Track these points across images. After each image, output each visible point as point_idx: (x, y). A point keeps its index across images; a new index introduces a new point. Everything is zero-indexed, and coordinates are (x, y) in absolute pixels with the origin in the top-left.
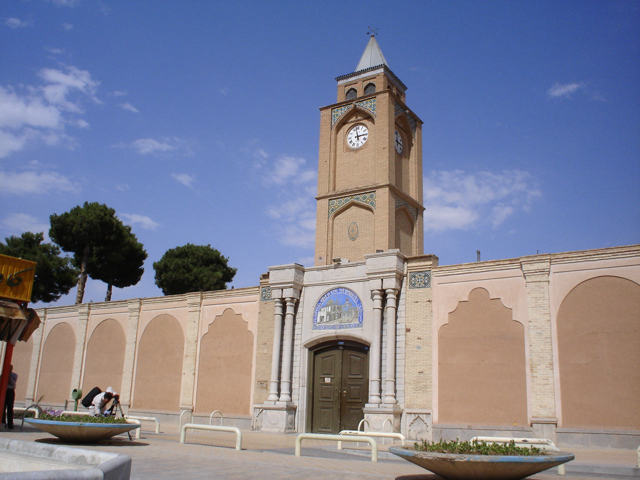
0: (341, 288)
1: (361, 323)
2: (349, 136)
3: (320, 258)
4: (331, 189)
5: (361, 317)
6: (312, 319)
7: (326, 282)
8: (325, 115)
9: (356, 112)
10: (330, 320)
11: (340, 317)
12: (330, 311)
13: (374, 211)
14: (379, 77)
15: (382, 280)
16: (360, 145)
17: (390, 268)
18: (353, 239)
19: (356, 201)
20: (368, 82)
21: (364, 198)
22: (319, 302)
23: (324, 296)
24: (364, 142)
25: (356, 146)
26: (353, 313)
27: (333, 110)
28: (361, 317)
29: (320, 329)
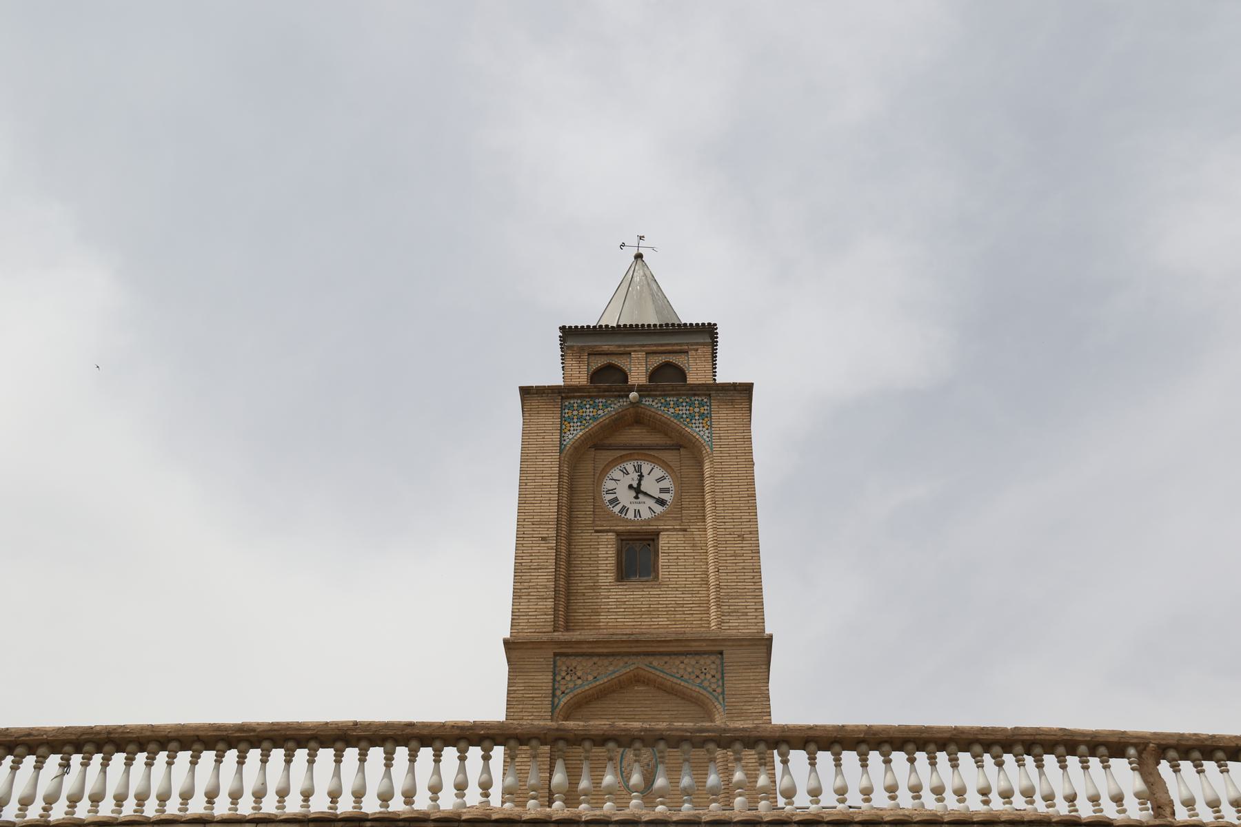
2: (609, 485)
20: (661, 359)
24: (659, 509)
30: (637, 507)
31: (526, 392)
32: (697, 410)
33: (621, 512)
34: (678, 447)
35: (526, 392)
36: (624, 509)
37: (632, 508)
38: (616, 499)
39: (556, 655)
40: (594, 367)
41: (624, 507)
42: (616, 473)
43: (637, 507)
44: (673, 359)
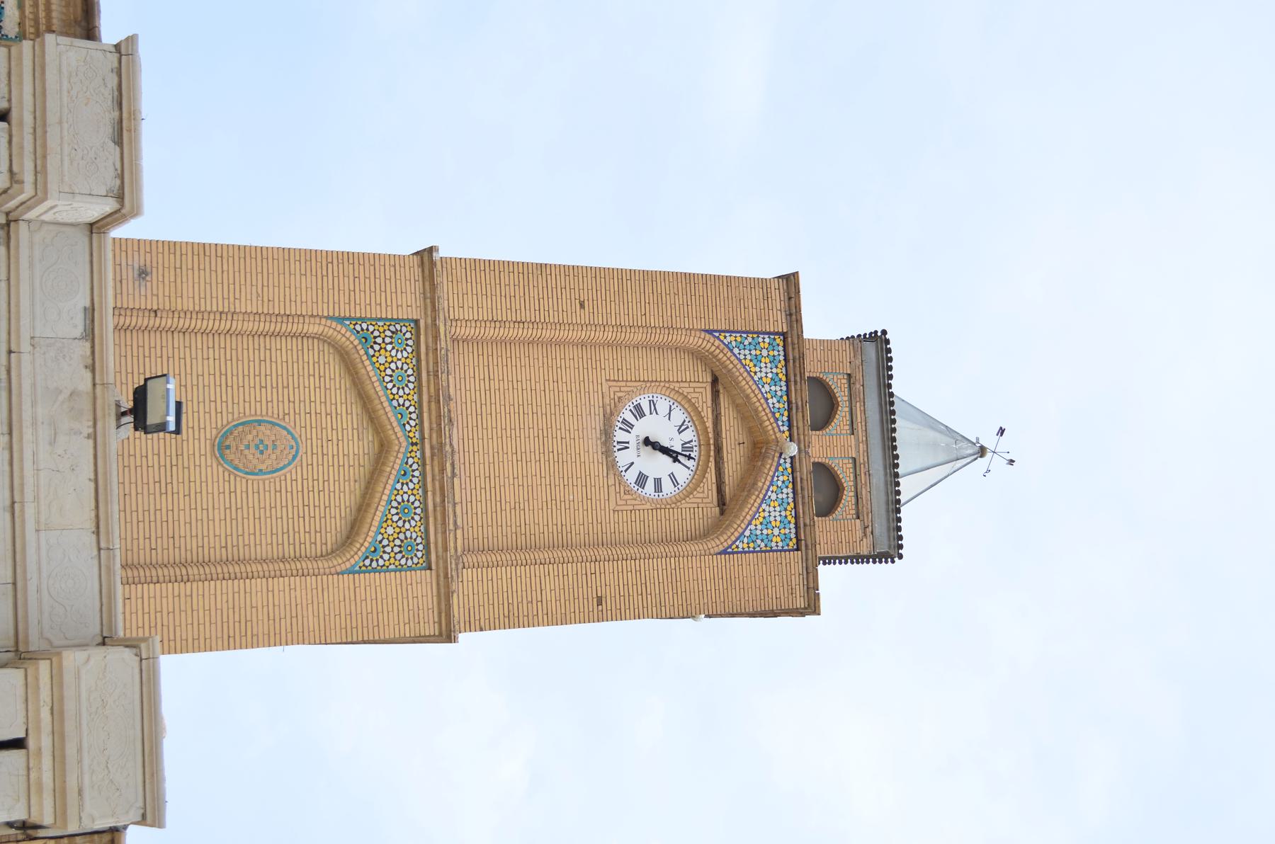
2: (663, 405)
3: (143, 273)
4: (462, 331)
7: (26, 358)
8: (767, 298)
9: (758, 450)
13: (340, 563)
14: (859, 533)
15: (18, 744)
16: (623, 458)
18: (221, 447)
19: (394, 465)
21: (403, 509)
24: (631, 477)
25: (620, 436)
27: (779, 340)
30: (633, 445)
31: (790, 282)
32: (776, 531)
33: (625, 421)
34: (722, 503)
35: (790, 282)
36: (628, 426)
37: (631, 438)
38: (642, 415)
39: (416, 322)
40: (831, 380)
41: (632, 426)
42: (679, 416)
43: (633, 445)
44: (848, 497)
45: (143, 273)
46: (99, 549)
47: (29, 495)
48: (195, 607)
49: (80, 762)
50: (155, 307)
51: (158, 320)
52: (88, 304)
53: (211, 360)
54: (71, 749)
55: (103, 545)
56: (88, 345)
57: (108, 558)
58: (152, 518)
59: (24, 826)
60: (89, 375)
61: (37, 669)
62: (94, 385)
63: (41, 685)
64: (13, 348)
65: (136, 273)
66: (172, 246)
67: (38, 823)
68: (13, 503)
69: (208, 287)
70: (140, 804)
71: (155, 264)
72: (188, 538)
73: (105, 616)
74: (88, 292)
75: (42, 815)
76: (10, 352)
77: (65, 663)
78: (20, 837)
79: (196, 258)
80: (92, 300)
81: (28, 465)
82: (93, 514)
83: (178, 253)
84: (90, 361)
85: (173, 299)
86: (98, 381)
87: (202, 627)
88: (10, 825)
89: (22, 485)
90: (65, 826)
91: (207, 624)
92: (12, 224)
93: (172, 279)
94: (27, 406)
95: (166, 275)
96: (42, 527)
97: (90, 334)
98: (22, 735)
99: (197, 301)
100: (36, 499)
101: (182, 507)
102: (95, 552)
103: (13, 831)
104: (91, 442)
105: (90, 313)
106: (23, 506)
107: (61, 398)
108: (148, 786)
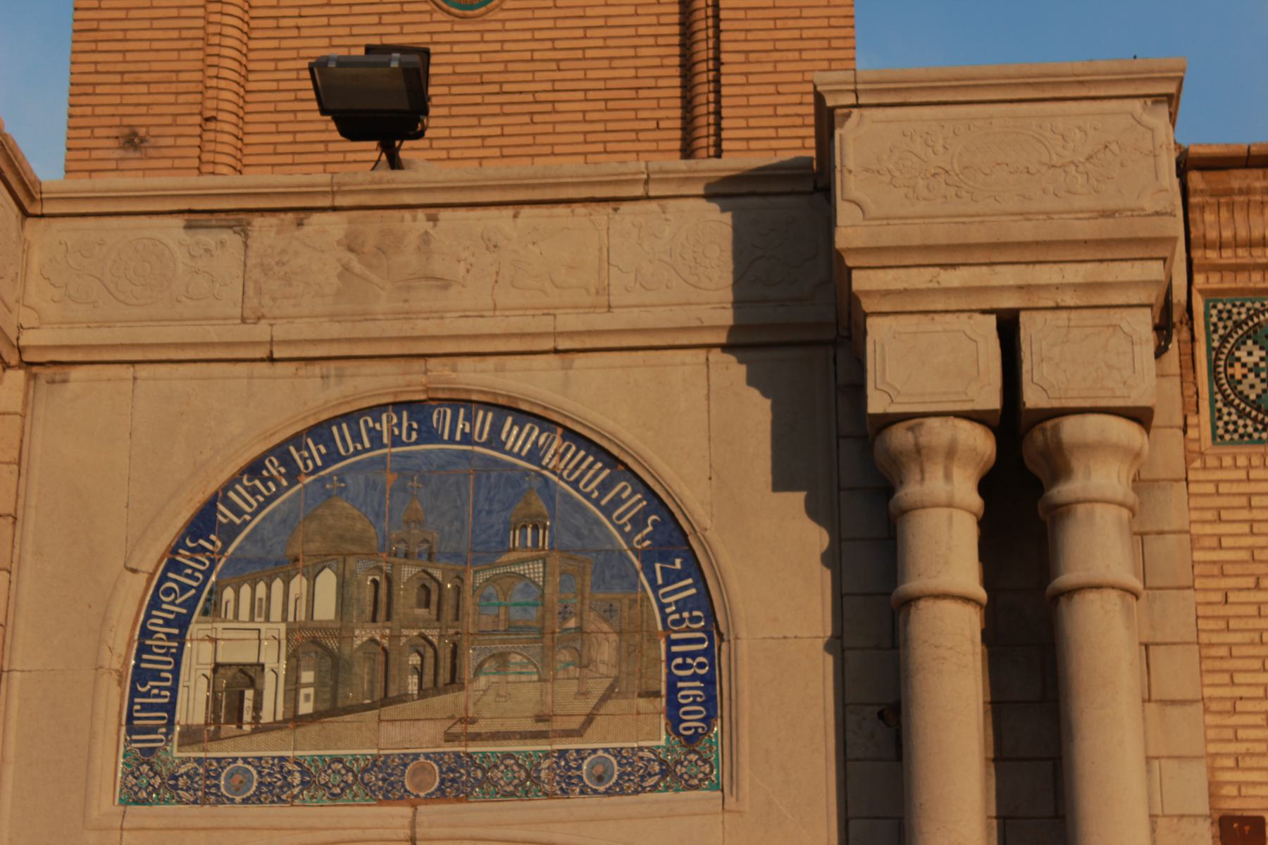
0: (462, 403)
1: (691, 741)
3: (132, 141)
5: (690, 690)
6: (113, 699)
7: (280, 332)
10: (330, 710)
11: (447, 675)
12: (326, 608)
15: (1008, 327)
17: (1106, 214)
22: (203, 523)
23: (254, 468)
26: (605, 651)
28: (690, 690)
29: (210, 795)
45: (132, 141)
46: (648, 198)
47: (545, 324)
48: (769, 46)
49: (1048, 214)
50: (198, 119)
51: (221, 116)
52: (179, 221)
53: (301, 22)
54: (1026, 231)
55: (639, 191)
56: (258, 221)
57: (662, 181)
58: (600, 127)
59: (1163, 329)
60: (316, 218)
61: (868, 293)
62: (334, 209)
63: (900, 286)
64: (262, 353)
65: (131, 154)
66: (80, 90)
67: (1163, 291)
68: (556, 351)
69: (156, 24)
70: (1137, 105)
71: (116, 121)
72: (639, 62)
73: (774, 188)
74: (156, 221)
75: (1145, 284)
76: (271, 359)
77: (858, 243)
78: (1185, 335)
79: (102, 46)
80: (171, 213)
81: (484, 326)
82: (580, 209)
83: (93, 79)
84: (290, 216)
85: (182, 87)
86: (326, 202)
87: (806, 34)
88: (1160, 352)
89: (522, 335)
90: (1174, 240)
91: (802, 23)
92: (27, 358)
93: (143, 89)
94: (373, 329)
95: (134, 100)
96: (603, 300)
97: (236, 218)
98: (992, 319)
99: (186, 44)
100: (550, 311)
101: (580, 74)
102: (653, 205)
103: (1173, 346)
104: (444, 214)
105: (196, 218)
106: (562, 334)
107: (357, 266)
108: (1102, 93)
